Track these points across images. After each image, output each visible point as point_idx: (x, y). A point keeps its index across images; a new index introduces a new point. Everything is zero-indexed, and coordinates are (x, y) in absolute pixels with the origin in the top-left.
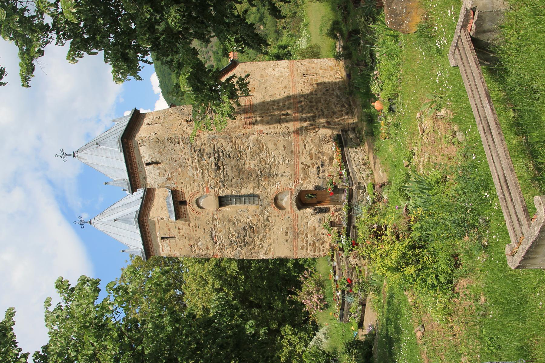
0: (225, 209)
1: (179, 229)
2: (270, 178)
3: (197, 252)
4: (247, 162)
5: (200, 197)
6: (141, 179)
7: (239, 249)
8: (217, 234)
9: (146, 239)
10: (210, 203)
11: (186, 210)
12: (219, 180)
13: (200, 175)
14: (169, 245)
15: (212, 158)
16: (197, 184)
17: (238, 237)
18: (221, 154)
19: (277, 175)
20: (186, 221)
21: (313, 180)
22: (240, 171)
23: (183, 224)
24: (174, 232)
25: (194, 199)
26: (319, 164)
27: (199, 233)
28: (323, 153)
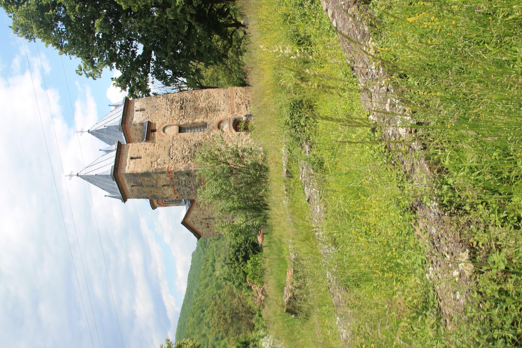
0: (182, 134)
1: (146, 149)
2: (215, 112)
3: (156, 166)
4: (200, 104)
5: (166, 127)
6: (130, 118)
7: (190, 162)
8: (174, 151)
9: (119, 158)
10: (172, 131)
11: (154, 135)
12: (181, 114)
13: (169, 112)
14: (135, 163)
15: (179, 104)
16: (166, 118)
17: (189, 152)
18: (185, 101)
19: (219, 110)
20: (152, 142)
21: (243, 112)
22: (196, 109)
23: (150, 145)
24: (142, 154)
25: (162, 127)
26: (247, 103)
27: (161, 151)
28: (248, 97)
